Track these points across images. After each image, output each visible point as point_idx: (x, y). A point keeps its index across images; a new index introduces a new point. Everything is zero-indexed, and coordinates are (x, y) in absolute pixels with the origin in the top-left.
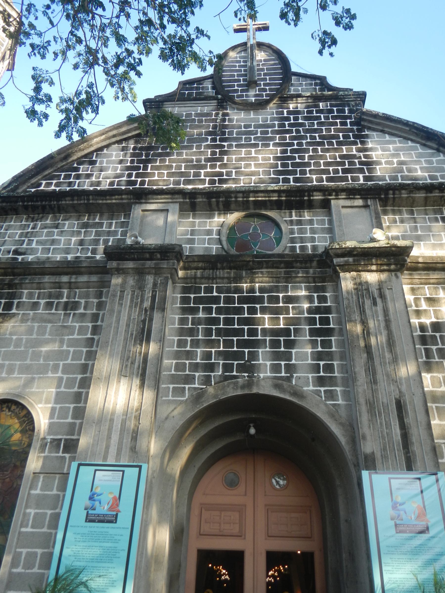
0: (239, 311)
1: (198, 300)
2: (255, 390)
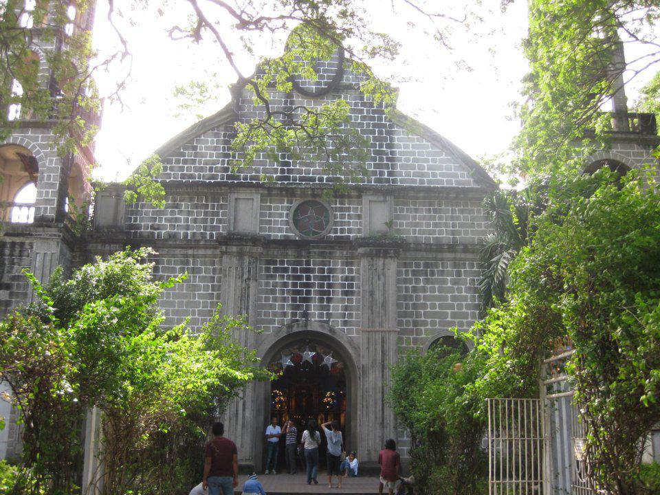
1: (276, 270)
2: (309, 329)
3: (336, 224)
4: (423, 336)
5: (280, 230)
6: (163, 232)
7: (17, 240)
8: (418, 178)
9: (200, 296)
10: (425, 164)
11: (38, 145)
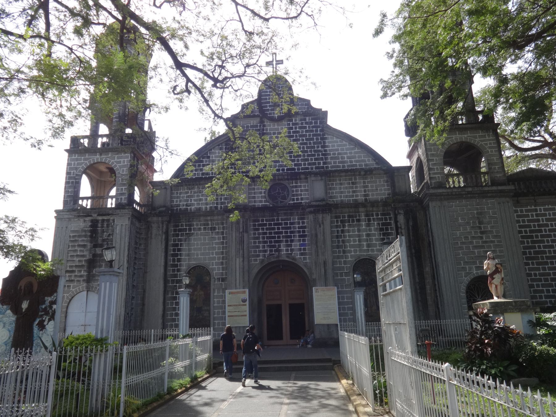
0: (274, 229)
1: (259, 225)
2: (280, 259)
3: (293, 195)
4: (350, 259)
5: (261, 201)
6: (193, 207)
7: (105, 218)
8: (341, 165)
9: (216, 243)
10: (345, 156)
11: (115, 161)
